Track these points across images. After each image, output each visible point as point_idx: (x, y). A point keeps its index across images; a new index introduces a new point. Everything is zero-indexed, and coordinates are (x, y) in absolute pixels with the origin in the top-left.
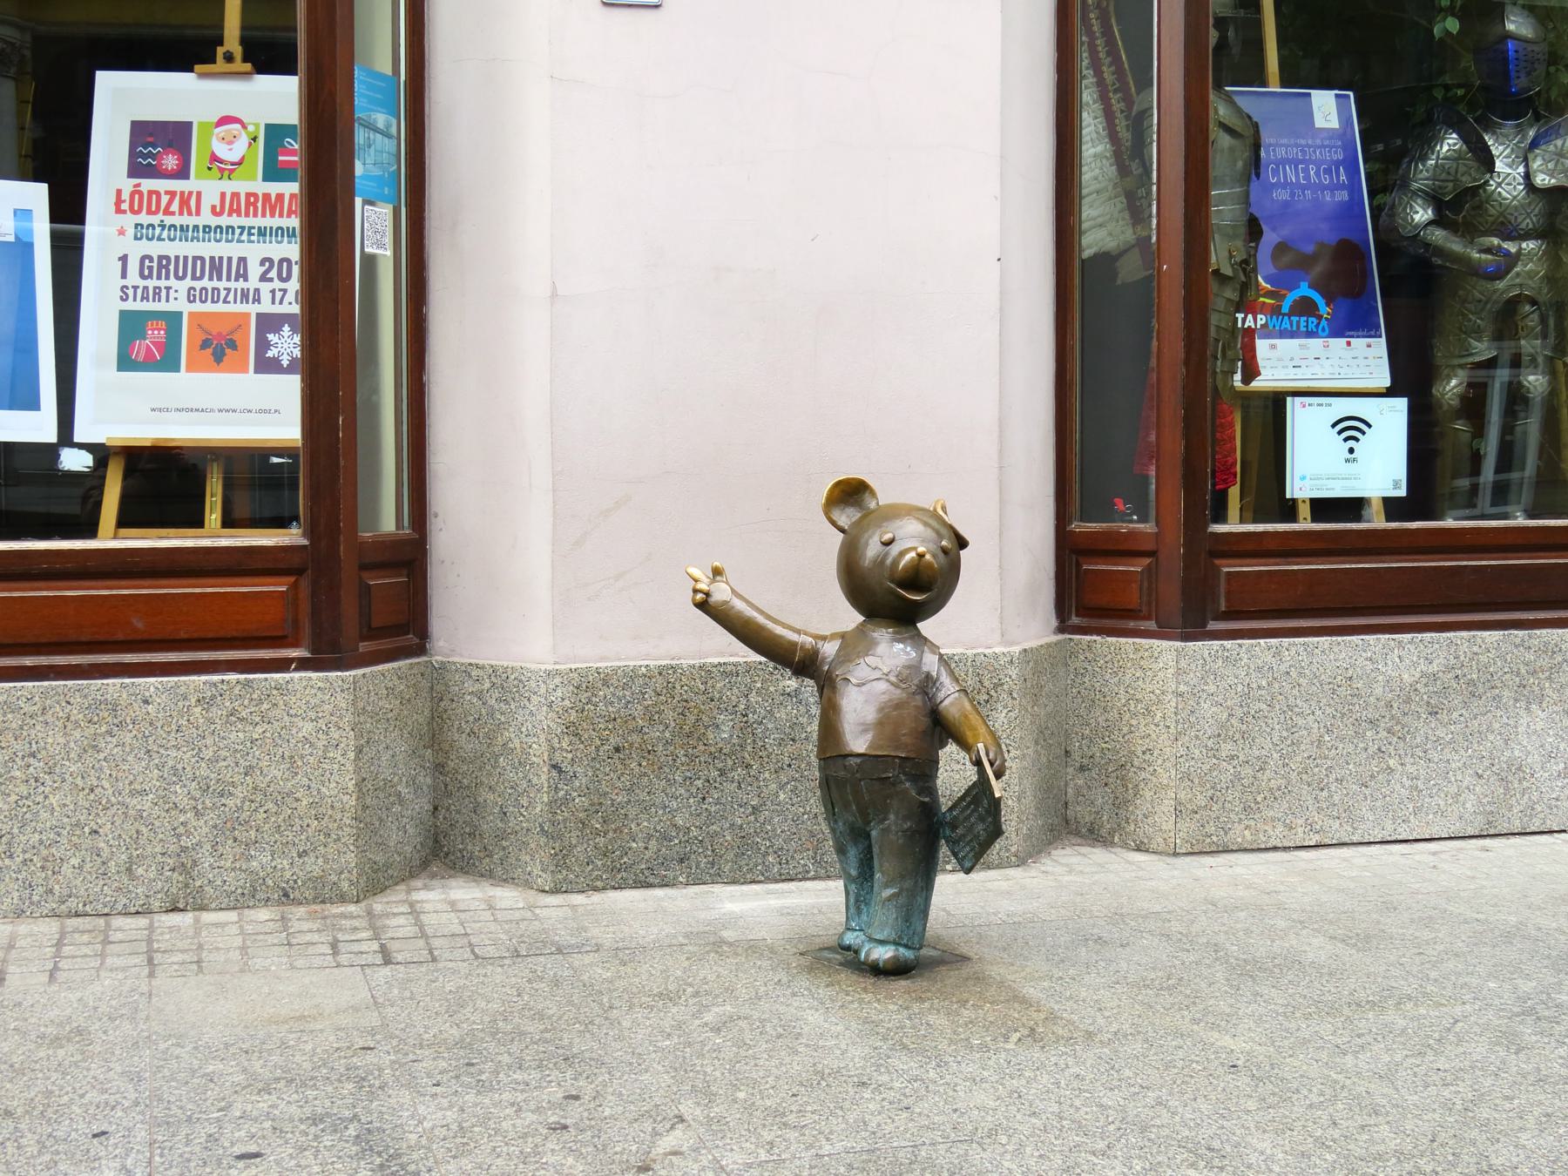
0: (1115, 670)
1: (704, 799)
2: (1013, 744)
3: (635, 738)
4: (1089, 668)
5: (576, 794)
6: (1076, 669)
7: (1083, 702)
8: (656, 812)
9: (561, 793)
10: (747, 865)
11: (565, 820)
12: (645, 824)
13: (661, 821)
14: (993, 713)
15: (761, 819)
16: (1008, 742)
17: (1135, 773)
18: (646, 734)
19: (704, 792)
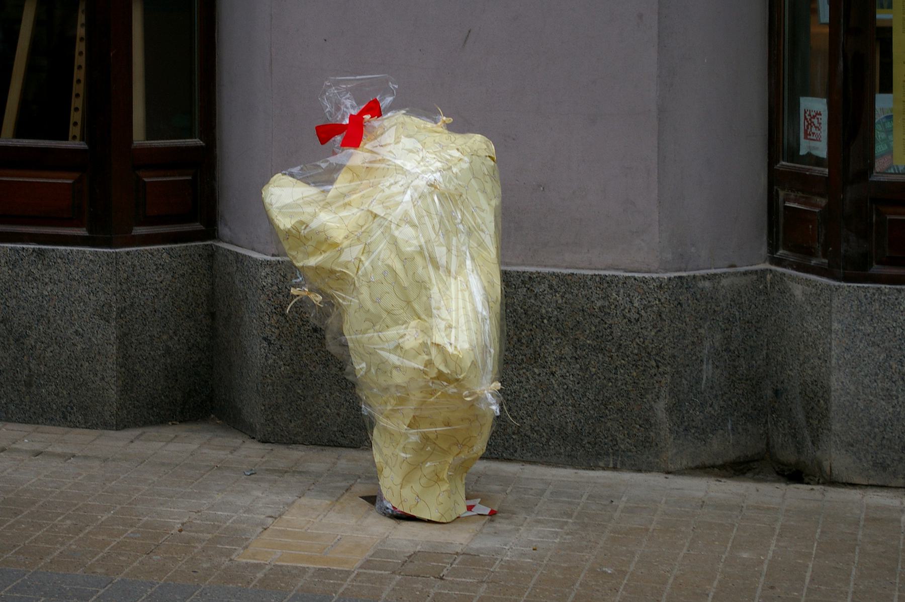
2: (663, 361)
5: (282, 363)
9: (271, 361)
11: (273, 384)
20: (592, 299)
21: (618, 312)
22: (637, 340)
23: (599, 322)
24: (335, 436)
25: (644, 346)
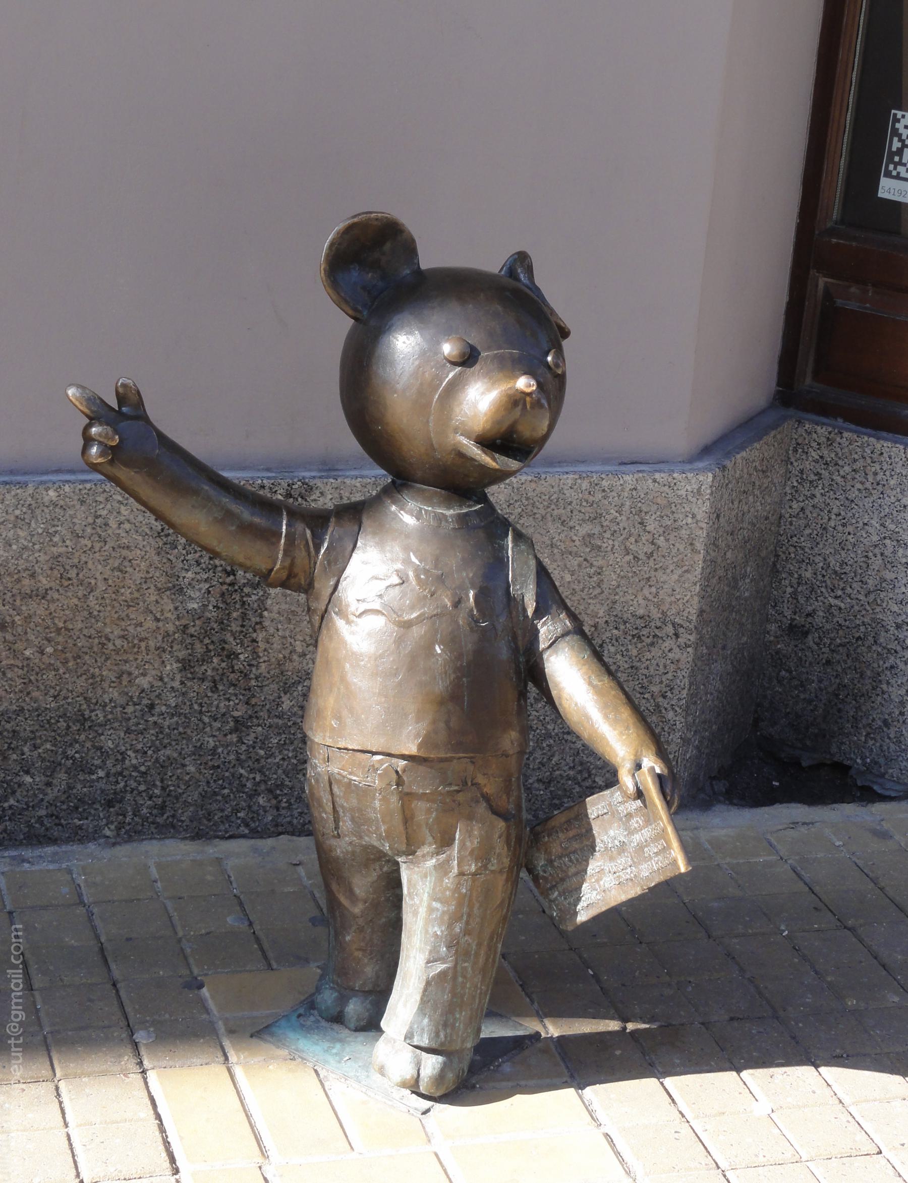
0: (868, 485)
1: (151, 707)
3: (38, 608)
6: (802, 472)
8: (68, 727)
10: (222, 810)
13: (77, 741)
14: (660, 573)
15: (249, 740)
17: (879, 654)
18: (53, 600)
19: (153, 696)
20: (571, 524)
21: (616, 544)
22: (646, 592)
23: (580, 565)
24: (42, 824)
25: (656, 600)
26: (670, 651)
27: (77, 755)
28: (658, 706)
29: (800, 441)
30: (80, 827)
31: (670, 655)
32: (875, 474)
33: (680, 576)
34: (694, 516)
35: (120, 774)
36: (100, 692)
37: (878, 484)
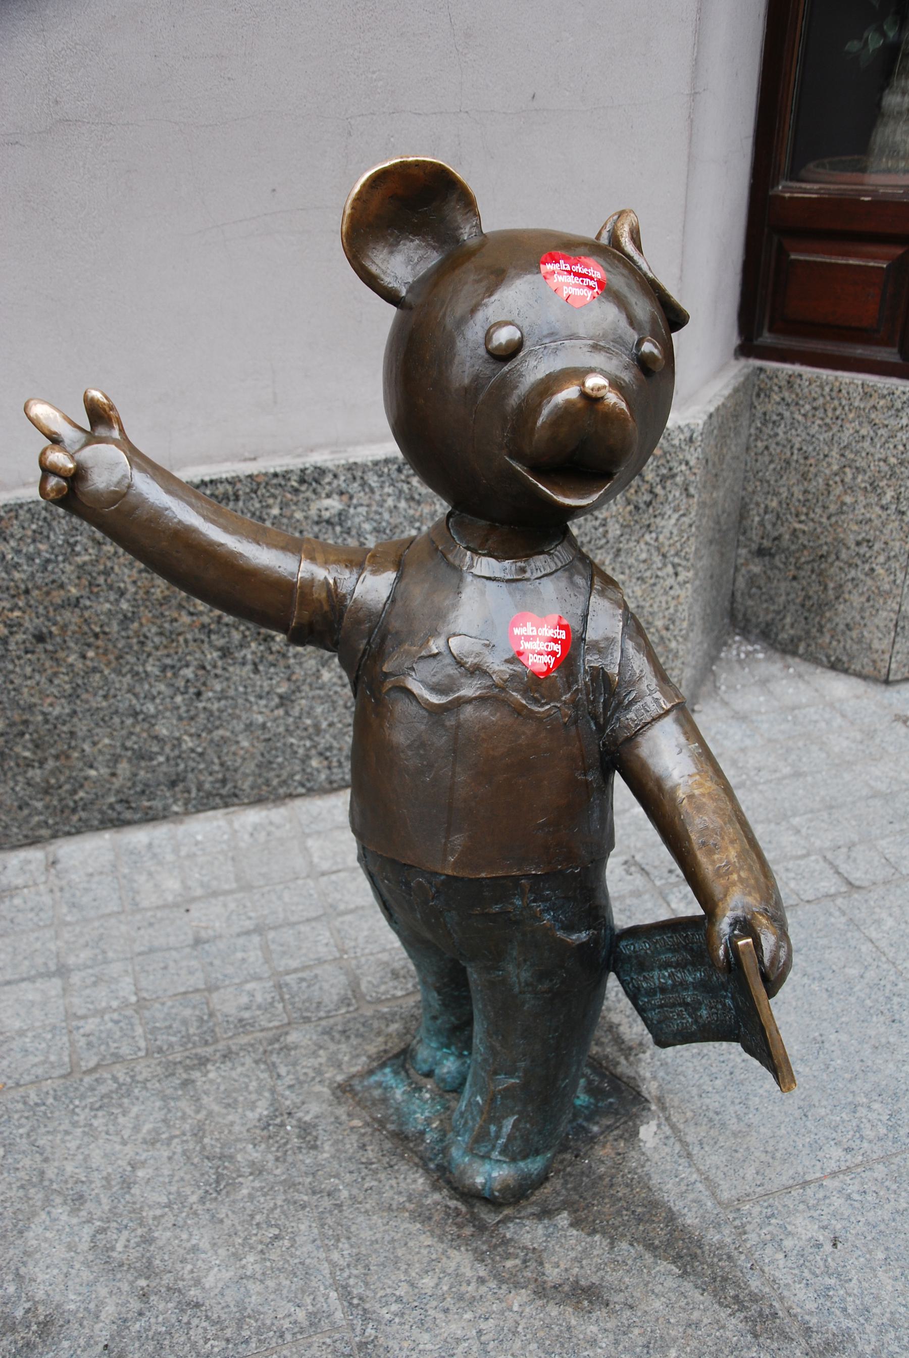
0: (828, 421)
1: (199, 694)
2: (684, 563)
3: (69, 616)
4: (787, 414)
7: (771, 462)
8: (122, 722)
12: (107, 741)
13: (131, 733)
14: (658, 520)
15: (296, 712)
16: (676, 560)
17: (841, 569)
18: (87, 608)
19: (198, 684)
22: (647, 537)
26: (671, 588)
27: (136, 747)
28: (662, 638)
29: (762, 386)
30: (150, 808)
31: (672, 592)
32: (835, 409)
33: (678, 520)
34: (687, 463)
35: (179, 757)
36: (146, 687)
37: (837, 418)
